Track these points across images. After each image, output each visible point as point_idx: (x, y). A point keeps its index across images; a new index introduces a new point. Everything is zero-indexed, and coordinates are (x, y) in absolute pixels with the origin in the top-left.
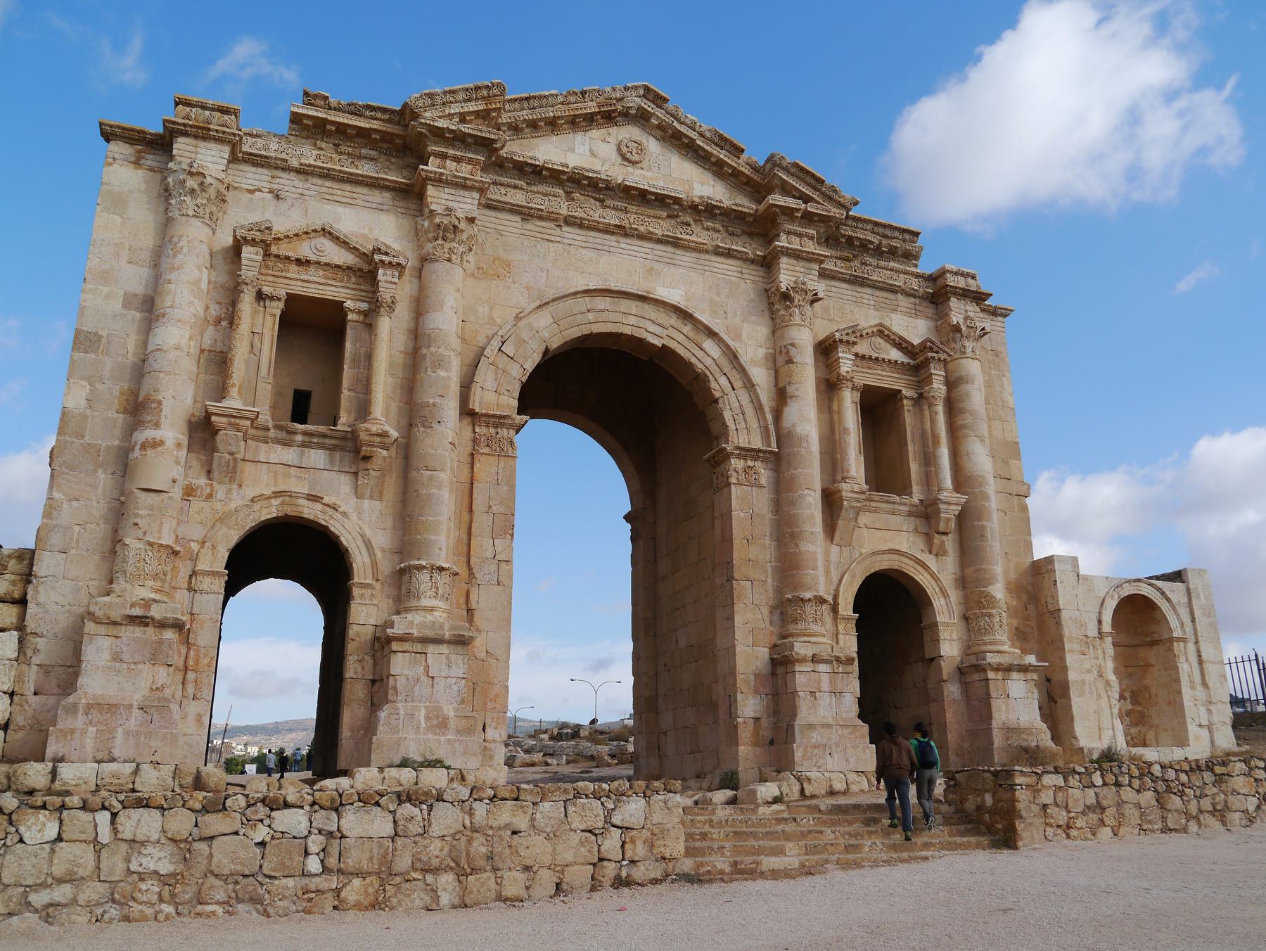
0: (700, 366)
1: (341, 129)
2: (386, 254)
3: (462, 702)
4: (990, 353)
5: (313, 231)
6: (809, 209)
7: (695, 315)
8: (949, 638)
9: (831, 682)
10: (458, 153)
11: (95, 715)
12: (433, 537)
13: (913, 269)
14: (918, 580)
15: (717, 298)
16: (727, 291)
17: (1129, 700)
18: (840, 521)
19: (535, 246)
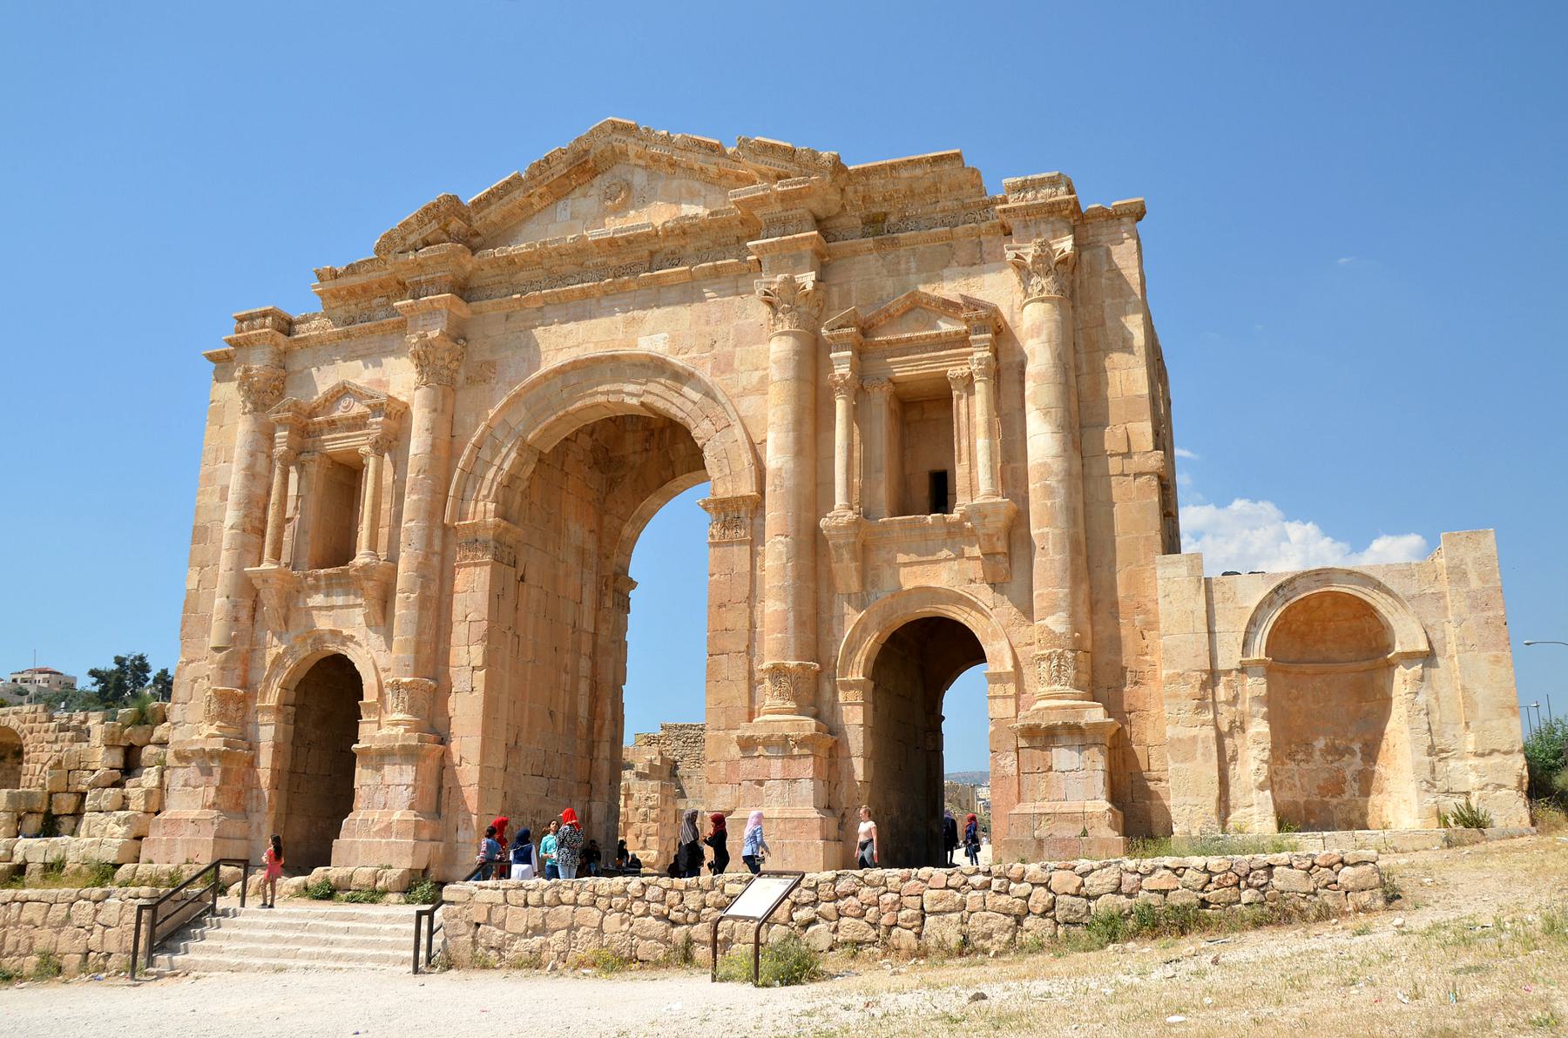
0: (680, 414)
1: (351, 292)
2: (372, 397)
3: (411, 807)
4: (1110, 275)
5: (338, 392)
6: (779, 189)
7: (668, 359)
8: (1001, 693)
9: (783, 767)
10: (429, 277)
11: (169, 828)
12: (401, 655)
13: (977, 199)
14: (962, 621)
15: (708, 329)
16: (718, 315)
17: (1359, 755)
18: (833, 565)
19: (518, 337)
